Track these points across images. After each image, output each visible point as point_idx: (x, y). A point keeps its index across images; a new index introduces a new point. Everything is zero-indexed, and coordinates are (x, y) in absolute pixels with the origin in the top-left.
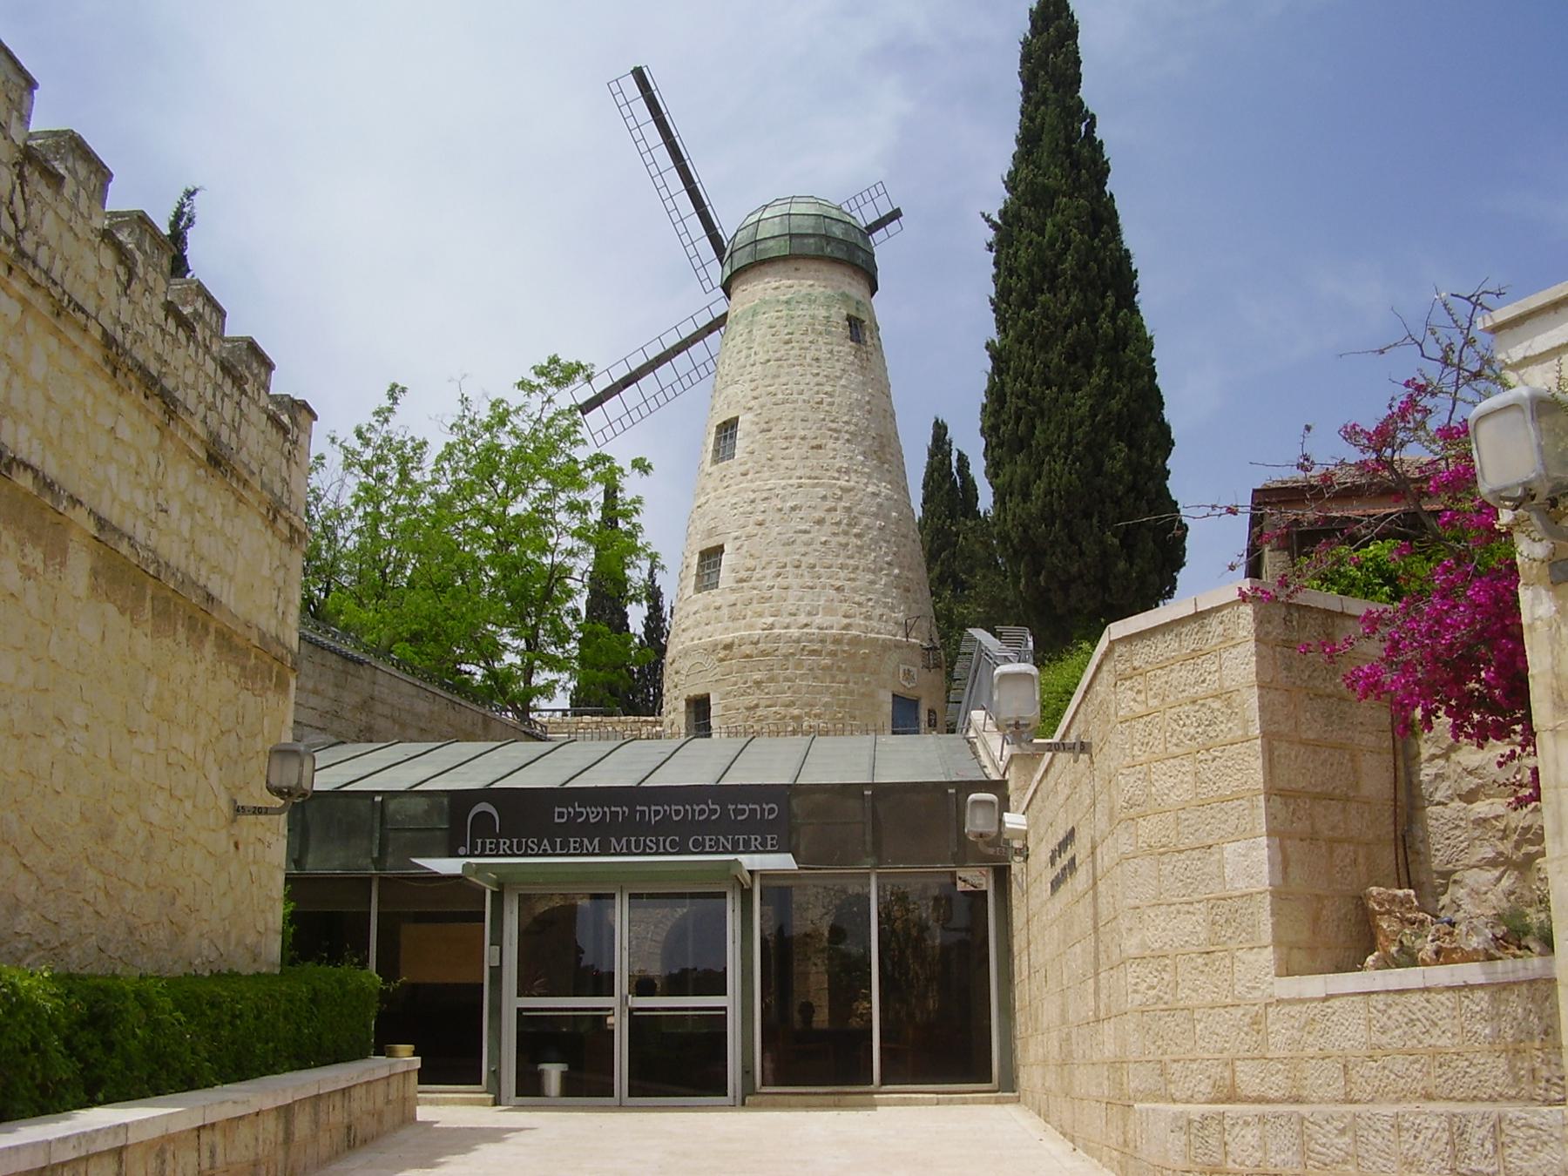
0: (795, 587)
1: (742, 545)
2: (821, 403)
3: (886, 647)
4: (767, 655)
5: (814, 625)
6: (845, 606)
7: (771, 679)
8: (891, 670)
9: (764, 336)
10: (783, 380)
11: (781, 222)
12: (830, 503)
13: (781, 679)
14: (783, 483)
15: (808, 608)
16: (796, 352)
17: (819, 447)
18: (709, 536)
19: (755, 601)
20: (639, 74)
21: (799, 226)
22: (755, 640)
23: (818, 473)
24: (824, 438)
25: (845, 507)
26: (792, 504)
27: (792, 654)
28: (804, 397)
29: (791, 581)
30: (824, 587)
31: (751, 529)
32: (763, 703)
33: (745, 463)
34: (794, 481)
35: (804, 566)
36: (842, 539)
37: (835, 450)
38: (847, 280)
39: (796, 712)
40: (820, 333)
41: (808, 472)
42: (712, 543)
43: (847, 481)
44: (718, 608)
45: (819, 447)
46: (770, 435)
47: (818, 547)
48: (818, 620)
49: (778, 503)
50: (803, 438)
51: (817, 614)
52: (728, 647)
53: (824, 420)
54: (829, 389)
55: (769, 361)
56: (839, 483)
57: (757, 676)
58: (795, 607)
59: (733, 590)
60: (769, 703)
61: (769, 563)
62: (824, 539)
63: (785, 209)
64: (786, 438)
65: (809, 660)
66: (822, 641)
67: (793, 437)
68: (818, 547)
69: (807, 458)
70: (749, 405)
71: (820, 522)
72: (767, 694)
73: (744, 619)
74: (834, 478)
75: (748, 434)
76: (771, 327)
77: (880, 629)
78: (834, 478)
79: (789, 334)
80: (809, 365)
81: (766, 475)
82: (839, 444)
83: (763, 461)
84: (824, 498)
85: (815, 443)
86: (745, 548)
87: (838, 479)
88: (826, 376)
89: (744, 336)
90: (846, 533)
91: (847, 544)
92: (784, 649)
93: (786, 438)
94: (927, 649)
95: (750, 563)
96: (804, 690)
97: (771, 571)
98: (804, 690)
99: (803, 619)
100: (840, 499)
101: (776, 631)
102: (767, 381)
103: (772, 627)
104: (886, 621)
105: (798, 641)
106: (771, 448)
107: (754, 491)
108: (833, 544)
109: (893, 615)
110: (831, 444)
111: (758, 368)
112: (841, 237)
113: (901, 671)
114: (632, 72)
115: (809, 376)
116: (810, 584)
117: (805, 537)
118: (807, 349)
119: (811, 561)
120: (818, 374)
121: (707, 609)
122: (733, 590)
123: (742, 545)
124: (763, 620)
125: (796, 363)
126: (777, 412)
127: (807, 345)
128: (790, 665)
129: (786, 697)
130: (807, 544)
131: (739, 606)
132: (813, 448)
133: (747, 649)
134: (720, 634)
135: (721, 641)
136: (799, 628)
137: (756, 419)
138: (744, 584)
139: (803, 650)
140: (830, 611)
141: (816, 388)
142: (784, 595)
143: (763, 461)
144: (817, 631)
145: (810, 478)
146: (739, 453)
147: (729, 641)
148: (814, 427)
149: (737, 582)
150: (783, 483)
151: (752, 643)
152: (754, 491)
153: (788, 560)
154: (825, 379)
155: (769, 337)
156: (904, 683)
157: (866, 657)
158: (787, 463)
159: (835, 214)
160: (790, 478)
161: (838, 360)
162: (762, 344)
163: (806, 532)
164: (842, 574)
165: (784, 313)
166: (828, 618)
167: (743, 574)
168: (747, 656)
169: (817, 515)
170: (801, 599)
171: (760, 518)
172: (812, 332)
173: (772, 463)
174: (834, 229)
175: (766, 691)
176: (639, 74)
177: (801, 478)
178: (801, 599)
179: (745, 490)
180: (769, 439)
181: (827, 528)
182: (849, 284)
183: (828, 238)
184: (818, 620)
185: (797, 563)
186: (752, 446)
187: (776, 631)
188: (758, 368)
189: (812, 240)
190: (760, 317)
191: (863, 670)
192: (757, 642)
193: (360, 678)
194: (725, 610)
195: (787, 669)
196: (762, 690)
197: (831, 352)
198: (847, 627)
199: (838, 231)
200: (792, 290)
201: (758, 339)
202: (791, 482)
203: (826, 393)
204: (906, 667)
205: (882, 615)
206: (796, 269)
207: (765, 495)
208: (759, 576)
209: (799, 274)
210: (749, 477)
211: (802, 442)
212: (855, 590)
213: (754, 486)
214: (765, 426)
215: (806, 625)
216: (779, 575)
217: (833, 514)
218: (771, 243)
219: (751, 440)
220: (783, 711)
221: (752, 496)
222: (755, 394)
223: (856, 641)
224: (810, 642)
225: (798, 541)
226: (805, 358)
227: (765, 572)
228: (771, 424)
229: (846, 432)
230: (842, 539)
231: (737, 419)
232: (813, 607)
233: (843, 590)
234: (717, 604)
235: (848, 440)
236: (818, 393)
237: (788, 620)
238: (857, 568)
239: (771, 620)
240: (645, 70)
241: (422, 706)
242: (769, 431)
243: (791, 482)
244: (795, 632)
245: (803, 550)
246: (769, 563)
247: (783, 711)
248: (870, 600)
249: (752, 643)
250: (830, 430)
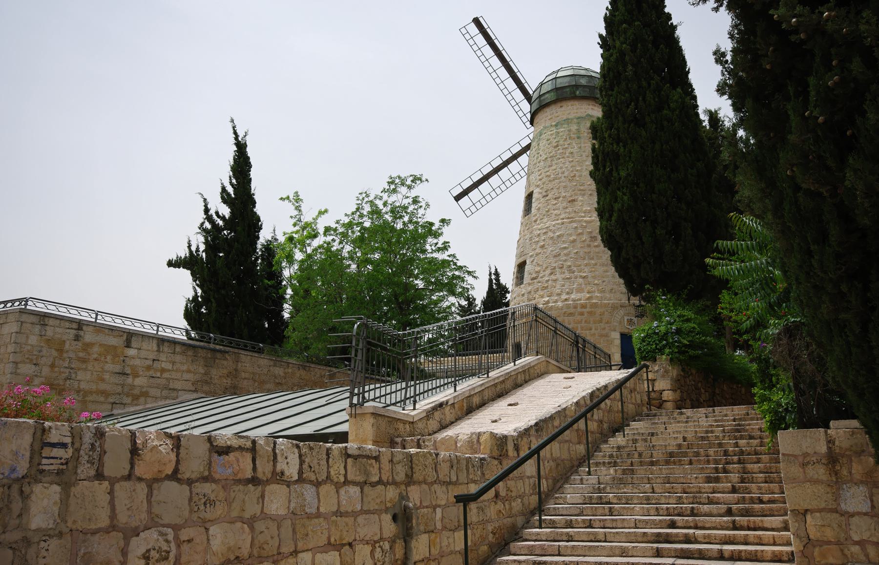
0: (560, 279)
1: (534, 260)
2: (575, 176)
3: (614, 307)
5: (571, 299)
6: (589, 288)
8: (618, 320)
9: (544, 146)
10: (554, 167)
11: (552, 83)
14: (554, 223)
15: (567, 290)
16: (561, 151)
17: (573, 201)
18: (521, 257)
19: (540, 289)
20: (477, 22)
21: (561, 83)
23: (572, 215)
24: (575, 194)
25: (588, 232)
26: (558, 234)
29: (559, 276)
30: (576, 277)
31: (538, 251)
33: (536, 215)
34: (560, 221)
36: (587, 250)
37: (582, 201)
38: (591, 107)
40: (574, 139)
41: (567, 215)
42: (521, 260)
43: (590, 217)
44: (523, 295)
45: (573, 201)
46: (548, 198)
47: (573, 255)
48: (573, 296)
49: (550, 234)
50: (564, 197)
51: (571, 293)
53: (576, 185)
54: (578, 168)
55: (546, 158)
56: (585, 219)
58: (560, 290)
59: (529, 284)
61: (547, 268)
63: (554, 76)
64: (555, 199)
66: (575, 307)
67: (559, 198)
68: (573, 255)
69: (567, 208)
70: (538, 184)
71: (574, 241)
73: (535, 299)
74: (582, 217)
75: (537, 199)
76: (548, 140)
77: (610, 297)
78: (582, 217)
79: (557, 142)
80: (568, 157)
81: (545, 220)
82: (586, 197)
83: (544, 212)
84: (576, 228)
86: (535, 261)
87: (584, 217)
88: (577, 161)
89: (536, 147)
90: (589, 246)
91: (590, 252)
93: (555, 199)
94: (637, 306)
95: (538, 269)
97: (548, 272)
99: (564, 297)
100: (585, 227)
101: (550, 305)
102: (547, 169)
103: (548, 302)
104: (615, 292)
105: (562, 308)
106: (548, 205)
107: (539, 230)
108: (581, 253)
109: (620, 289)
110: (580, 198)
111: (542, 163)
112: (585, 84)
113: (626, 320)
114: (473, 21)
115: (568, 163)
117: (565, 252)
118: (566, 148)
119: (569, 264)
120: (572, 161)
121: (519, 296)
122: (529, 284)
123: (534, 260)
124: (544, 299)
125: (560, 157)
126: (550, 186)
127: (566, 146)
130: (565, 255)
131: (533, 293)
132: (569, 202)
136: (562, 302)
137: (541, 191)
138: (535, 281)
139: (565, 313)
140: (580, 290)
141: (571, 169)
142: (554, 284)
143: (544, 212)
145: (568, 218)
146: (533, 210)
149: (532, 280)
150: (554, 223)
152: (539, 230)
154: (577, 163)
155: (547, 145)
156: (628, 327)
157: (602, 314)
158: (556, 211)
159: (583, 72)
160: (558, 220)
161: (584, 152)
162: (543, 150)
163: (565, 248)
164: (586, 270)
165: (555, 131)
166: (579, 294)
167: (534, 275)
170: (563, 286)
171: (542, 244)
172: (569, 139)
173: (549, 213)
174: (581, 81)
176: (477, 22)
177: (563, 219)
178: (563, 286)
179: (536, 229)
180: (547, 200)
182: (592, 109)
183: (577, 86)
184: (573, 296)
186: (539, 205)
187: (550, 305)
188: (542, 163)
189: (568, 90)
190: (543, 136)
191: (601, 321)
193: (226, 359)
194: (526, 296)
197: (580, 148)
198: (589, 298)
199: (583, 82)
200: (559, 118)
201: (542, 148)
202: (557, 222)
203: (577, 171)
204: (629, 318)
205: (612, 289)
206: (561, 107)
207: (544, 231)
208: (542, 275)
209: (562, 109)
210: (537, 223)
211: (564, 199)
212: (594, 277)
213: (539, 227)
214: (545, 194)
215: (566, 300)
216: (551, 274)
217: (581, 236)
218: (547, 95)
219: (539, 202)
221: (539, 232)
222: (540, 177)
223: (595, 305)
225: (562, 254)
226: (565, 154)
227: (544, 273)
229: (590, 190)
230: (587, 250)
231: (533, 192)
232: (570, 289)
233: (588, 278)
234: (523, 293)
235: (591, 195)
236: (572, 171)
237: (556, 298)
238: (596, 264)
239: (547, 299)
240: (481, 19)
241: (279, 371)
242: (547, 196)
243: (557, 222)
244: (560, 304)
245: (564, 258)
246: (547, 268)
248: (604, 282)
250: (580, 190)
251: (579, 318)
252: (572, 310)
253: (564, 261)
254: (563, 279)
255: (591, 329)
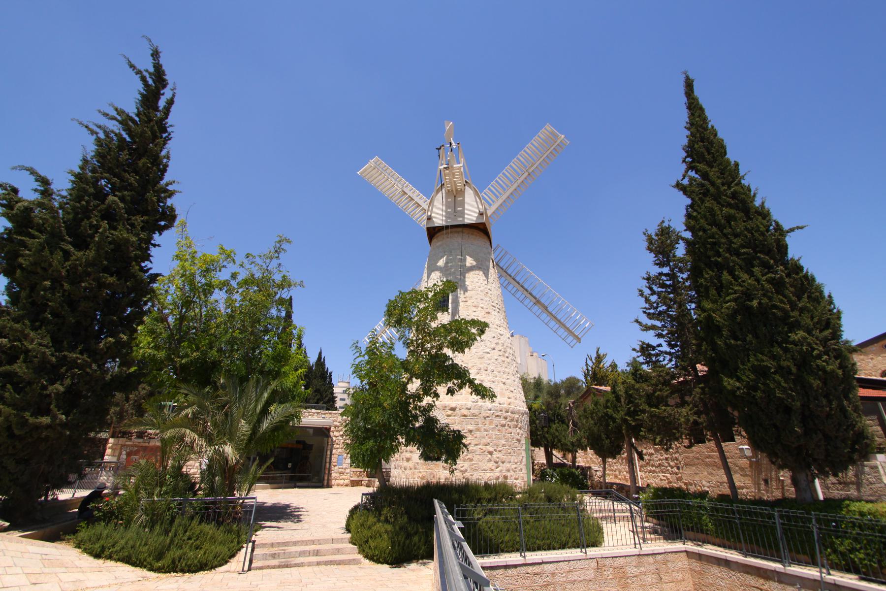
4: (476, 416)
7: (478, 430)
10: (472, 280)
12: (496, 341)
13: (482, 430)
17: (489, 313)
22: (469, 407)
27: (488, 417)
28: (481, 289)
30: (498, 382)
32: (474, 442)
35: (489, 370)
39: (491, 449)
46: (467, 304)
52: (453, 409)
57: (471, 428)
60: (476, 443)
62: (496, 358)
65: (496, 421)
67: (478, 307)
71: (494, 349)
72: (476, 437)
85: (487, 311)
92: (484, 414)
93: (475, 307)
96: (494, 437)
98: (494, 437)
116: (493, 380)
117: (489, 355)
128: (487, 423)
129: (485, 440)
133: (465, 412)
134: (448, 401)
135: (448, 406)
144: (499, 405)
147: (454, 406)
148: (486, 303)
151: (467, 408)
153: (482, 366)
164: (505, 376)
168: (465, 416)
169: (493, 345)
175: (475, 436)
181: (496, 352)
185: (486, 369)
192: (470, 409)
195: (485, 425)
196: (473, 435)
220: (484, 448)
224: (496, 410)
225: (486, 357)
228: (467, 299)
242: (466, 302)
247: (484, 448)
249: (467, 408)
251: (503, 422)
252: (499, 413)
253: (488, 364)
254: (489, 381)
255: (511, 433)
